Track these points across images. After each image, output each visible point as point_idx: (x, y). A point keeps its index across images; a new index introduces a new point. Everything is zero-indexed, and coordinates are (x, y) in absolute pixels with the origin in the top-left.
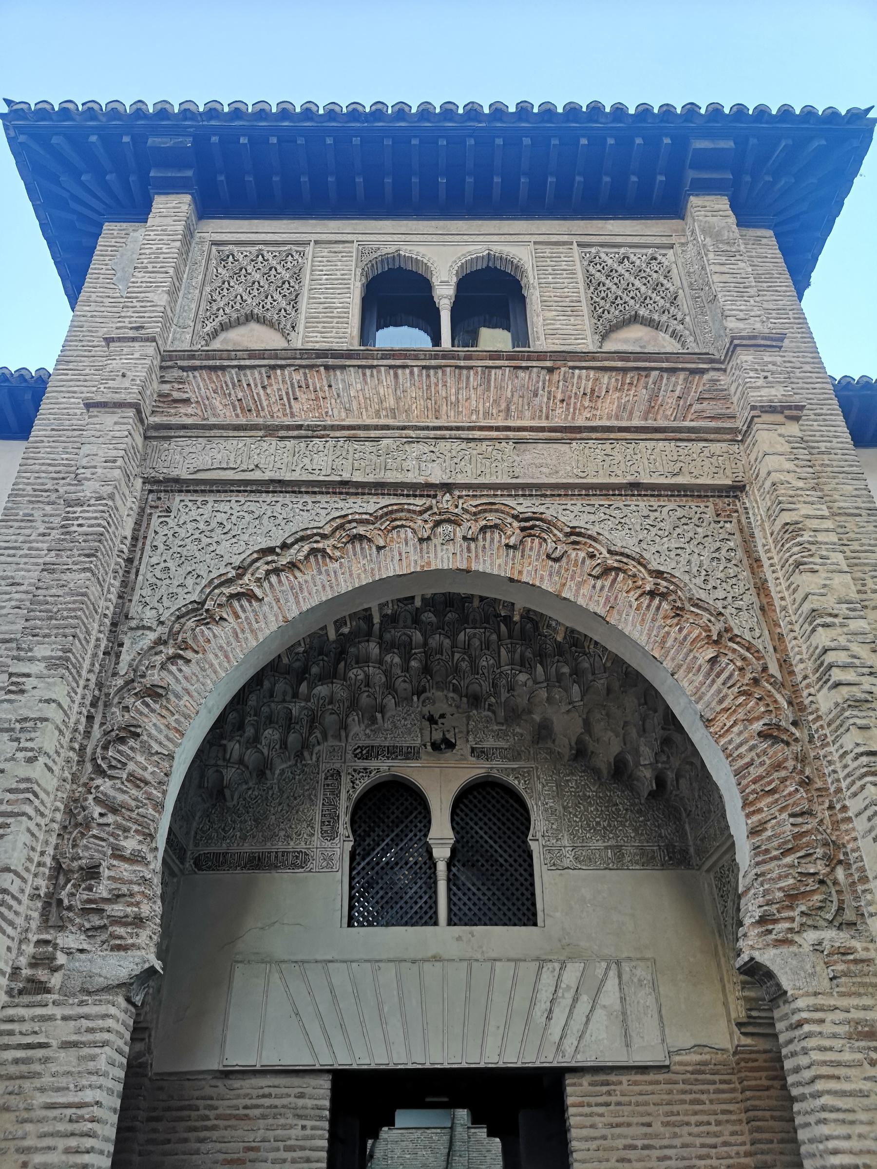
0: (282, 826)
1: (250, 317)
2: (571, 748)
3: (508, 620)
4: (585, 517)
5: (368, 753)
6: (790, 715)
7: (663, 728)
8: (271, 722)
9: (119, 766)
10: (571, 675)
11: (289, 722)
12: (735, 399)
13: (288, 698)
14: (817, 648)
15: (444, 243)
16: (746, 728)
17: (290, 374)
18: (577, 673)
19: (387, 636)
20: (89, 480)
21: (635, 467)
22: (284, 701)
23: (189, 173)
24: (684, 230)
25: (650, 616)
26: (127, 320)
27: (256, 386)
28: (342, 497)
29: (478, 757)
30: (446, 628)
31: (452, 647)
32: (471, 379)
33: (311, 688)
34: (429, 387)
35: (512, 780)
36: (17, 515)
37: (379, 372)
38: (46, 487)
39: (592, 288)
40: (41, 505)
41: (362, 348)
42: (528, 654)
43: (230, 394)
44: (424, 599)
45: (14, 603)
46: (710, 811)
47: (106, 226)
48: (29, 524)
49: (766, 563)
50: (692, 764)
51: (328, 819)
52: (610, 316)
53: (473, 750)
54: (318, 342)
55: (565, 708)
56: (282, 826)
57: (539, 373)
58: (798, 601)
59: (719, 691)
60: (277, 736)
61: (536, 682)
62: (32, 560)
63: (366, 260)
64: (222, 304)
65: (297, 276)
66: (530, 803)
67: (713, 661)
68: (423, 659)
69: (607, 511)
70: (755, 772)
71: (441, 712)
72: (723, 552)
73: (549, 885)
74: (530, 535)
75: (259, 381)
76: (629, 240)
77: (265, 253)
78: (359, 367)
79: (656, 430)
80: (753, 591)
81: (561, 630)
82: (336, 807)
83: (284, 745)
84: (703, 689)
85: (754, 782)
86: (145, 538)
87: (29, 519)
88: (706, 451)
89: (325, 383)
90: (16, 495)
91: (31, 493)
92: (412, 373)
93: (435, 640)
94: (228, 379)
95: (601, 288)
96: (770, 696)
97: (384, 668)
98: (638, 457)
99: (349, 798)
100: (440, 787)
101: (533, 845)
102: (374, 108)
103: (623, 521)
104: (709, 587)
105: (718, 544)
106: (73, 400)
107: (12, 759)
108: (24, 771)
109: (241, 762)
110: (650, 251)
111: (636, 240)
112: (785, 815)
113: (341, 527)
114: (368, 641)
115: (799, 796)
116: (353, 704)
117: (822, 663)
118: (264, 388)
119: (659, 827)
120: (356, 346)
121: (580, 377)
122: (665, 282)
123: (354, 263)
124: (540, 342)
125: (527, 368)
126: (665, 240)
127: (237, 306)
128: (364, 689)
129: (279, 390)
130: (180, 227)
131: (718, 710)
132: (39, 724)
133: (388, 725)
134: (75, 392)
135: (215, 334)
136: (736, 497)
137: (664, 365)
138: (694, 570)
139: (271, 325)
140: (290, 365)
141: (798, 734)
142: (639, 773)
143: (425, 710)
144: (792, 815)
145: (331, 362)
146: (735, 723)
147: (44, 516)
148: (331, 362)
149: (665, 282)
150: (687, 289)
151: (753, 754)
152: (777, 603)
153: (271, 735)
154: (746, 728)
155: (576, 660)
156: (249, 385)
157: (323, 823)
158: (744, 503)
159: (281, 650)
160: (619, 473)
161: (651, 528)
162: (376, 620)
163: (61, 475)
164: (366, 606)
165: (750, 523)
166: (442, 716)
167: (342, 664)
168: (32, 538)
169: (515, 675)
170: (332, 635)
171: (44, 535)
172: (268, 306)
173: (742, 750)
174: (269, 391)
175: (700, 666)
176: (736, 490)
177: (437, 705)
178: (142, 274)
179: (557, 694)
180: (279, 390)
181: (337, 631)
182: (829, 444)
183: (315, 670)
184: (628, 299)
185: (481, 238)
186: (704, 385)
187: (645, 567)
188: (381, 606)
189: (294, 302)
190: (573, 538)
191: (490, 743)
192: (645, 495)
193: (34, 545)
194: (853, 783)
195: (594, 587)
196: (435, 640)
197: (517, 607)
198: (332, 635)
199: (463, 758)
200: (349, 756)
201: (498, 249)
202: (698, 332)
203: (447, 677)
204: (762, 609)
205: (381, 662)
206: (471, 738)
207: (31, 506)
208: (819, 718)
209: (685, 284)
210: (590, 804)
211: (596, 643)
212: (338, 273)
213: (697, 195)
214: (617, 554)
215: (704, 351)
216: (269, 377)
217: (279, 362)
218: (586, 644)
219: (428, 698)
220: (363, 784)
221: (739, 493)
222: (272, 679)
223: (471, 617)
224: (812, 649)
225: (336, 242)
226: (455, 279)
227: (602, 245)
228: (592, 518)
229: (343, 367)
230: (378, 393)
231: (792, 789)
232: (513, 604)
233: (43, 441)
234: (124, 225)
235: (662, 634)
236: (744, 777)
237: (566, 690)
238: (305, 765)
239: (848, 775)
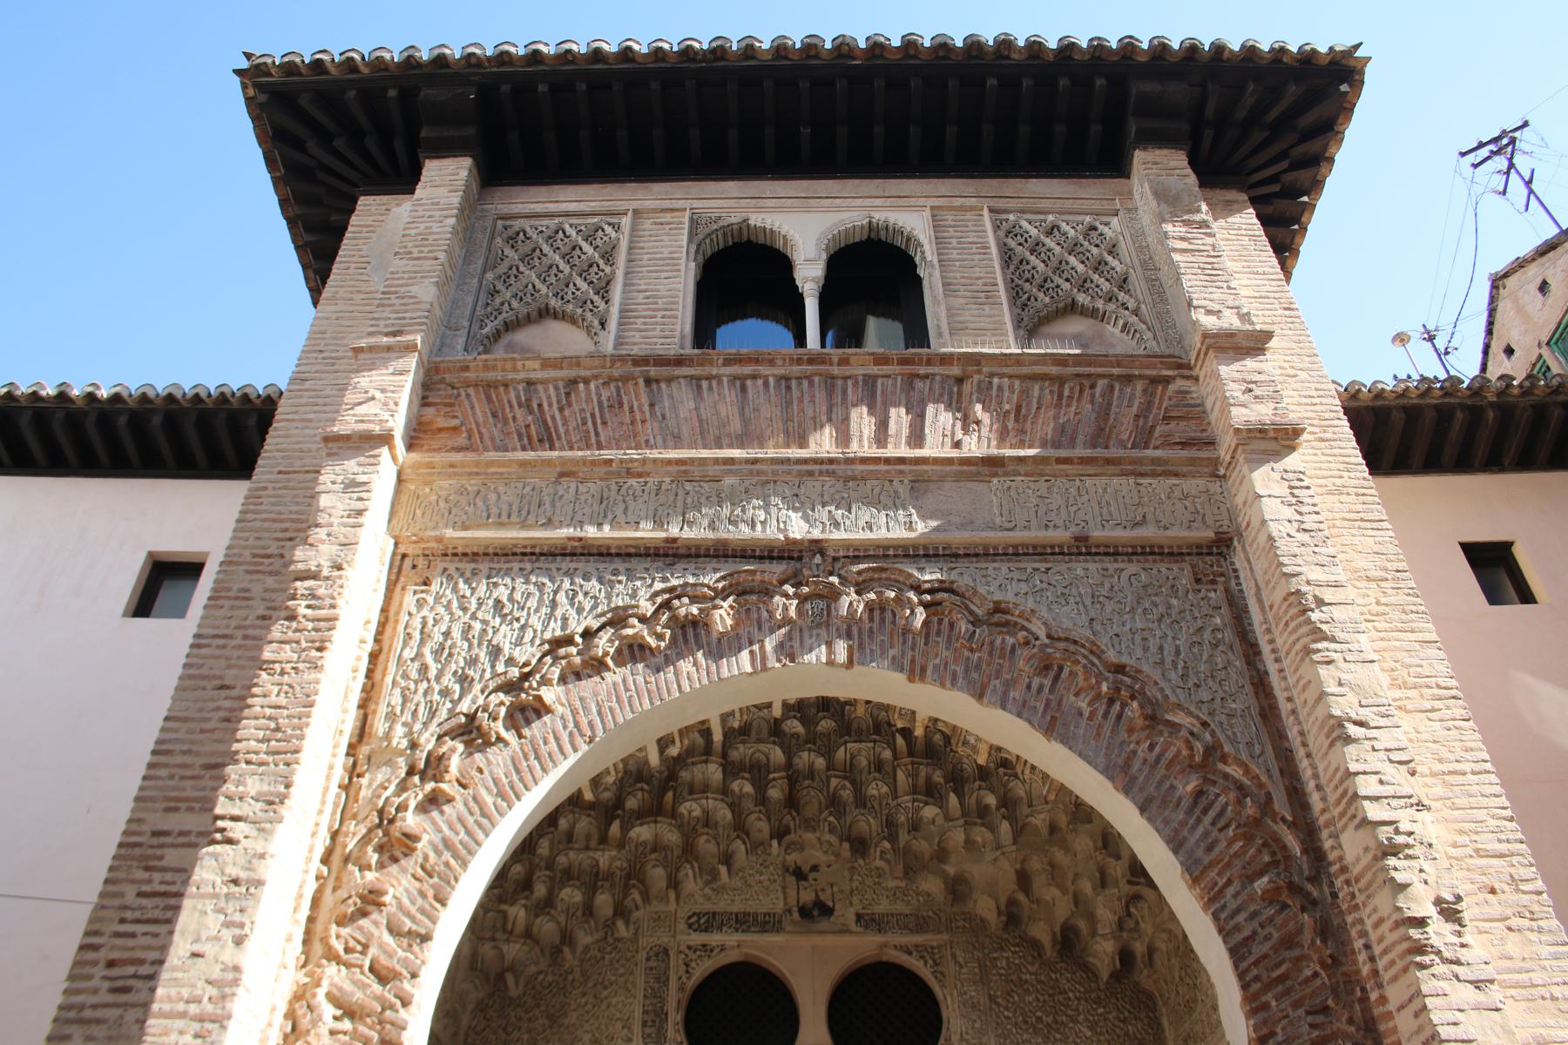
0: (587, 1027)
1: (545, 313)
2: (1000, 913)
3: (907, 733)
4: (1013, 588)
5: (707, 922)
6: (1305, 866)
7: (1129, 882)
8: (570, 878)
9: (359, 948)
10: (998, 808)
11: (593, 880)
12: (1213, 417)
13: (593, 844)
14: (1337, 770)
15: (808, 210)
16: (1244, 887)
17: (597, 387)
18: (1008, 803)
19: (734, 755)
20: (323, 542)
21: (1081, 514)
22: (587, 848)
23: (471, 131)
24: (1130, 193)
25: (1107, 731)
26: (382, 323)
27: (550, 405)
28: (668, 560)
29: (866, 927)
31: (828, 769)
32: (850, 391)
33: (625, 829)
34: (789, 403)
36: (229, 589)
37: (720, 383)
38: (268, 551)
39: (1012, 267)
40: (259, 576)
41: (697, 351)
42: (938, 777)
43: (514, 419)
44: (785, 704)
45: (222, 714)
46: (1195, 1001)
47: (362, 200)
48: (244, 603)
49: (1266, 649)
50: (1170, 931)
51: (651, 1016)
52: (1039, 305)
53: (859, 917)
54: (639, 344)
55: (989, 855)
56: (587, 1027)
57: (943, 382)
58: (1310, 702)
59: (1206, 834)
61: (948, 818)
62: (247, 653)
63: (702, 232)
64: (508, 295)
65: (609, 256)
67: (1199, 793)
68: (786, 788)
69: (1045, 578)
70: (1258, 950)
71: (813, 862)
72: (1207, 635)
74: (936, 614)
75: (554, 400)
76: (1059, 204)
77: (567, 227)
78: (692, 377)
79: (1109, 461)
80: (1249, 689)
81: (984, 749)
82: (663, 1000)
83: (589, 909)
84: (1185, 833)
85: (1256, 964)
86: (397, 621)
87: (244, 596)
88: (1177, 493)
89: (645, 400)
90: (230, 563)
91: (249, 559)
92: (766, 384)
93: (804, 758)
94: (513, 395)
95: (1023, 267)
96: (1276, 838)
97: (729, 800)
98: (1085, 498)
99: (682, 988)
100: (810, 969)
102: (714, 45)
103: (1066, 591)
104: (1190, 684)
105: (1199, 623)
106: (307, 431)
107: (217, 939)
108: (229, 954)
109: (528, 934)
110: (1088, 219)
111: (1068, 205)
112: (1301, 1012)
113: (666, 605)
114: (706, 762)
115: (1318, 982)
116: (689, 850)
117: (1345, 792)
118: (561, 410)
119: (1124, 1021)
120: (689, 350)
121: (1000, 388)
122: (1109, 259)
123: (685, 238)
124: (943, 342)
125: (927, 376)
126: (1106, 206)
127: (528, 299)
129: (582, 410)
130: (456, 199)
131: (1207, 859)
132: (252, 890)
134: (310, 420)
135: (497, 335)
136: (1220, 554)
137: (1116, 371)
138: (1168, 660)
139: (573, 321)
140: (596, 377)
141: (1315, 894)
142: (1096, 947)
144: (1308, 1013)
145: (653, 371)
146: (1229, 882)
147: (266, 590)
148: (653, 371)
149: (1109, 259)
150: (1139, 270)
151: (1255, 924)
152: (1284, 707)
153: (571, 895)
154: (1244, 887)
155: (1005, 786)
156: (540, 405)
157: (644, 1024)
158: (1232, 563)
159: (584, 783)
160: (1060, 523)
161: (1106, 602)
162: (718, 736)
163: (288, 535)
164: (702, 718)
165: (1241, 591)
166: (815, 868)
167: (670, 795)
168: (248, 622)
170: (654, 759)
171: (264, 618)
172: (570, 296)
173: (1241, 918)
174: (566, 413)
175: (1180, 799)
176: (1222, 544)
178: (404, 262)
179: (980, 834)
180: (582, 410)
181: (662, 751)
182: (1338, 482)
183: (632, 803)
184: (1061, 281)
185: (858, 202)
186: (1170, 399)
187: (1099, 658)
188: (725, 717)
189: (604, 290)
190: (997, 617)
191: (883, 907)
192: (1097, 554)
193: (251, 632)
194: (1393, 963)
195: (1029, 687)
196: (804, 758)
197: (919, 717)
198: (654, 759)
199: (845, 931)
200: (682, 926)
201: (879, 216)
202: (1157, 326)
203: (821, 812)
204: (1263, 715)
205: (725, 791)
206: (855, 900)
207: (249, 577)
208: (1344, 869)
209: (1137, 264)
211: (1033, 768)
212: (666, 251)
213: (1145, 149)
214: (1059, 639)
215: (1167, 352)
216: (568, 394)
217: (584, 373)
218: (1019, 769)
220: (703, 968)
221: (1224, 549)
222: (571, 817)
223: (855, 725)
224: (1331, 771)
225: (663, 211)
226: (824, 256)
227: (1023, 211)
228: (1024, 587)
229: (669, 380)
230: (718, 413)
231: (1308, 973)
232: (914, 713)
233: (265, 488)
234: (385, 198)
235: (1124, 755)
236: (1243, 958)
237: (992, 828)
238: (618, 940)
239: (1385, 952)
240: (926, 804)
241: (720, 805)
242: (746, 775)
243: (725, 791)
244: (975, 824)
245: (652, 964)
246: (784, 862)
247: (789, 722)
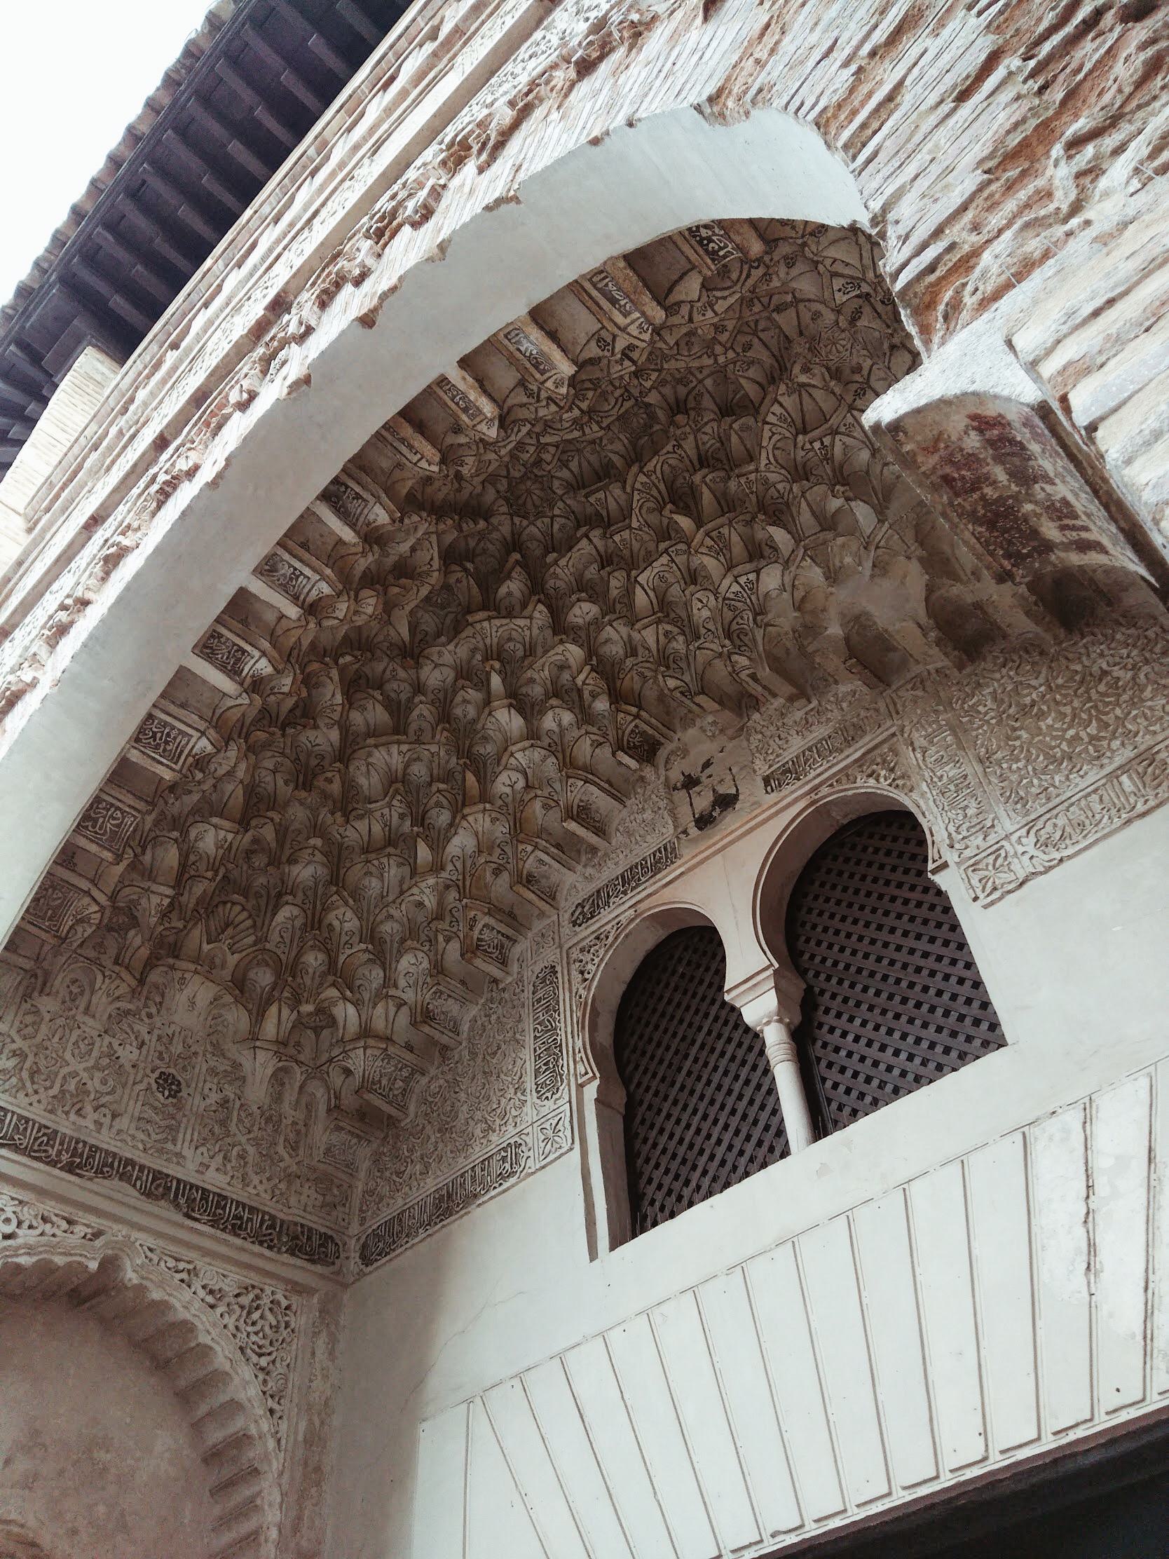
19: (537, 691)
30: (618, 606)
35: (864, 785)
53: (767, 780)
60: (426, 964)
66: (907, 801)
73: (1002, 941)
101: (942, 880)
109: (366, 1032)
128: (526, 798)
133: (617, 839)
143: (676, 776)
164: (229, 591)
166: (707, 764)
169: (753, 587)
177: (693, 753)
179: (844, 553)
200: (567, 929)
210: (1041, 715)
219: (672, 753)
237: (854, 530)
240: (758, 572)
241: (537, 754)
242: (554, 702)
243: (532, 734)
244: (825, 543)
245: (540, 994)
246: (667, 779)
247: (576, 610)
